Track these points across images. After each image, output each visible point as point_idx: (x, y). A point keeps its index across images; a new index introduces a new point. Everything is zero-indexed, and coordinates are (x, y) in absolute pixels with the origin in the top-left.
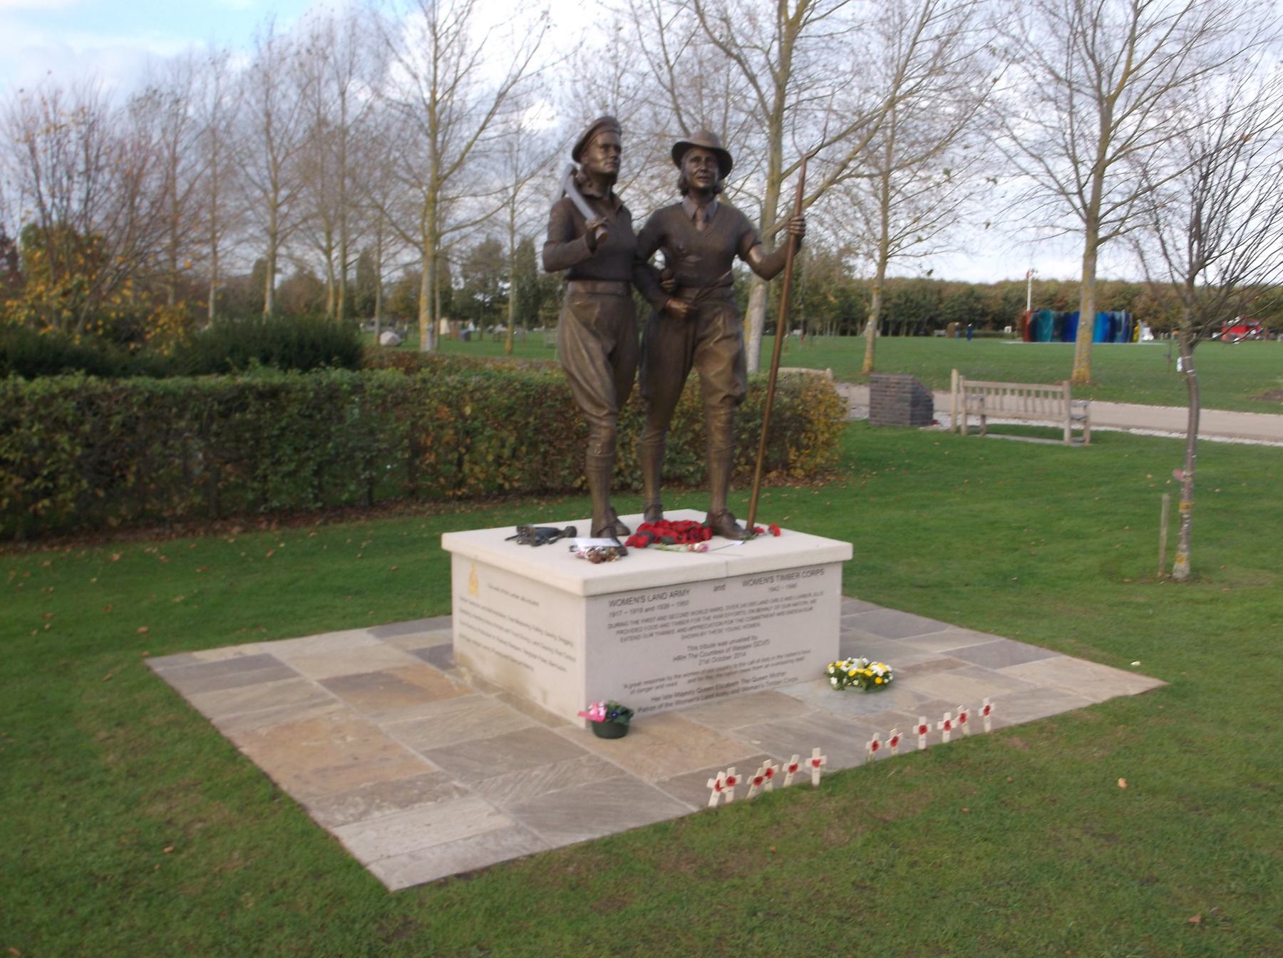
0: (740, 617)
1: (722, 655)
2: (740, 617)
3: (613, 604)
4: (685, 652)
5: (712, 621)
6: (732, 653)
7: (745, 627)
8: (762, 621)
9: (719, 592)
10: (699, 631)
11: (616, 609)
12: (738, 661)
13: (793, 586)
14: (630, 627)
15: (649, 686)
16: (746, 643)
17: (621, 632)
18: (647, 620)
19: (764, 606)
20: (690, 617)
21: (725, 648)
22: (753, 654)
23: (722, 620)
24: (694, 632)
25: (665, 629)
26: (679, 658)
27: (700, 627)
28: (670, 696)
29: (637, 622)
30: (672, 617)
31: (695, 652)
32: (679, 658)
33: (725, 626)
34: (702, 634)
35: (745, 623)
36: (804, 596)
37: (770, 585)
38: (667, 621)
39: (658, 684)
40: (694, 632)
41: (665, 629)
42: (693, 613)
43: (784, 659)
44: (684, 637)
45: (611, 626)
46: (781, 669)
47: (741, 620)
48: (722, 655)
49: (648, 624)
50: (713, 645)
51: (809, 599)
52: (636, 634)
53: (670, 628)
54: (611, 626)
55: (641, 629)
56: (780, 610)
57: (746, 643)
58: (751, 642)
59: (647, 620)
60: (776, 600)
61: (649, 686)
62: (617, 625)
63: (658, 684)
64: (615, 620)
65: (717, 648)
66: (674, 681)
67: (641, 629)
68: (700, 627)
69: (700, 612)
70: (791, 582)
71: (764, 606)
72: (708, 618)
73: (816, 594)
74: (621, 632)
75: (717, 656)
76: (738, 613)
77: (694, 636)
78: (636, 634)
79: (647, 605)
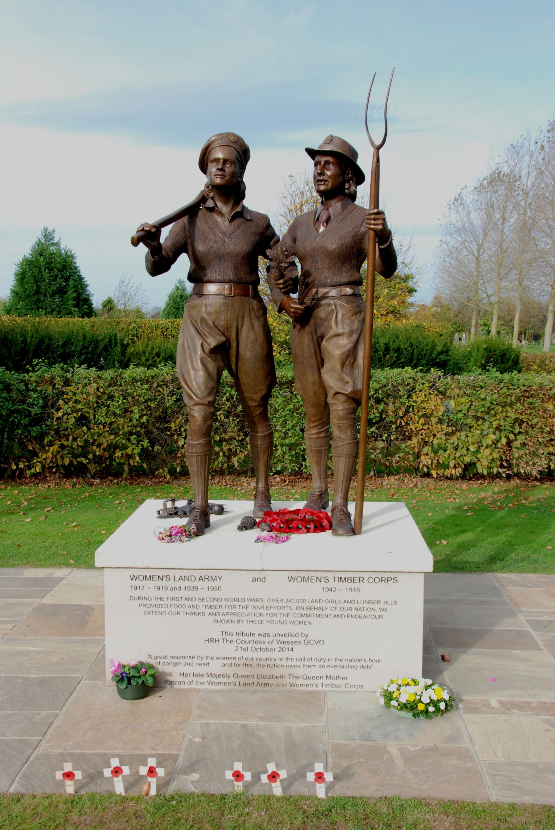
0: (285, 612)
1: (263, 646)
2: (285, 612)
3: (133, 578)
4: (219, 636)
5: (250, 610)
6: (275, 645)
7: (291, 622)
8: (312, 619)
9: (259, 583)
10: (235, 618)
11: (138, 583)
12: (283, 655)
13: (358, 590)
14: (154, 602)
15: (176, 661)
16: (294, 639)
17: (144, 605)
18: (172, 599)
19: (316, 605)
20: (223, 603)
21: (267, 639)
22: (300, 651)
23: (264, 611)
24: (228, 617)
25: (193, 610)
26: (210, 640)
27: (234, 614)
28: (201, 675)
29: (161, 599)
30: (202, 600)
31: (230, 638)
32: (210, 640)
33: (266, 618)
34: (238, 621)
35: (292, 619)
36: (369, 602)
37: (323, 584)
38: (197, 603)
39: (187, 661)
40: (228, 617)
41: (193, 610)
42: (226, 600)
43: (344, 663)
44: (216, 621)
45: (132, 598)
46: (342, 672)
47: (287, 615)
48: (263, 646)
49: (173, 602)
50: (253, 635)
51: (377, 606)
52: (161, 610)
53: (200, 610)
54: (132, 598)
55: (166, 606)
56: (338, 612)
57: (294, 639)
58: (300, 639)
59: (172, 599)
60: (331, 601)
61: (176, 661)
62: (139, 598)
63: (187, 661)
64: (136, 594)
65: (257, 638)
66: (205, 661)
67: (166, 606)
68: (234, 614)
69: (236, 600)
70: (352, 585)
71: (316, 605)
72: (246, 607)
73: (386, 602)
74: (144, 605)
75: (258, 646)
76: (283, 608)
77: (228, 621)
78: (161, 610)
79: (171, 584)
